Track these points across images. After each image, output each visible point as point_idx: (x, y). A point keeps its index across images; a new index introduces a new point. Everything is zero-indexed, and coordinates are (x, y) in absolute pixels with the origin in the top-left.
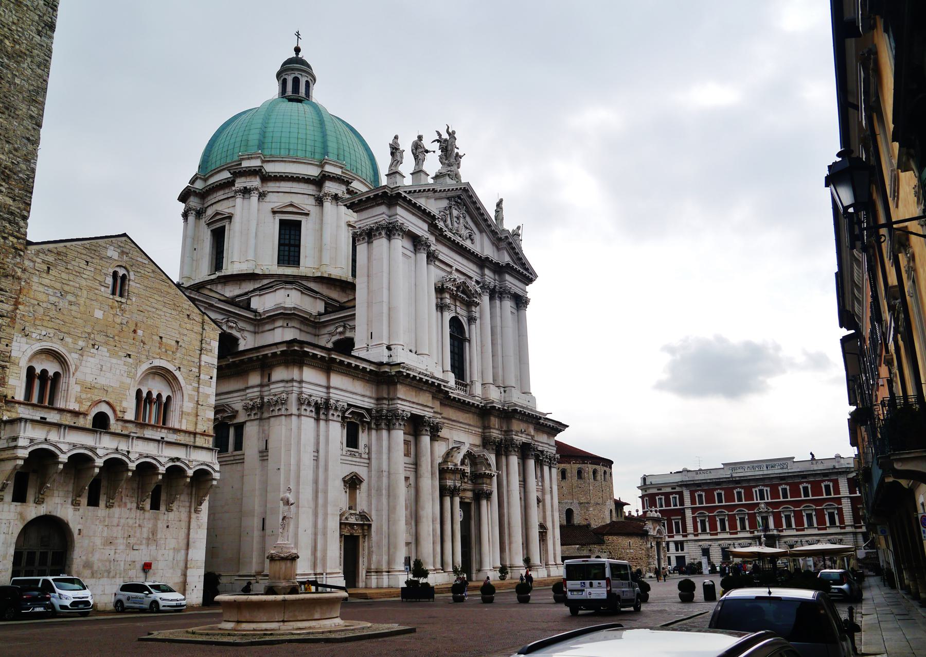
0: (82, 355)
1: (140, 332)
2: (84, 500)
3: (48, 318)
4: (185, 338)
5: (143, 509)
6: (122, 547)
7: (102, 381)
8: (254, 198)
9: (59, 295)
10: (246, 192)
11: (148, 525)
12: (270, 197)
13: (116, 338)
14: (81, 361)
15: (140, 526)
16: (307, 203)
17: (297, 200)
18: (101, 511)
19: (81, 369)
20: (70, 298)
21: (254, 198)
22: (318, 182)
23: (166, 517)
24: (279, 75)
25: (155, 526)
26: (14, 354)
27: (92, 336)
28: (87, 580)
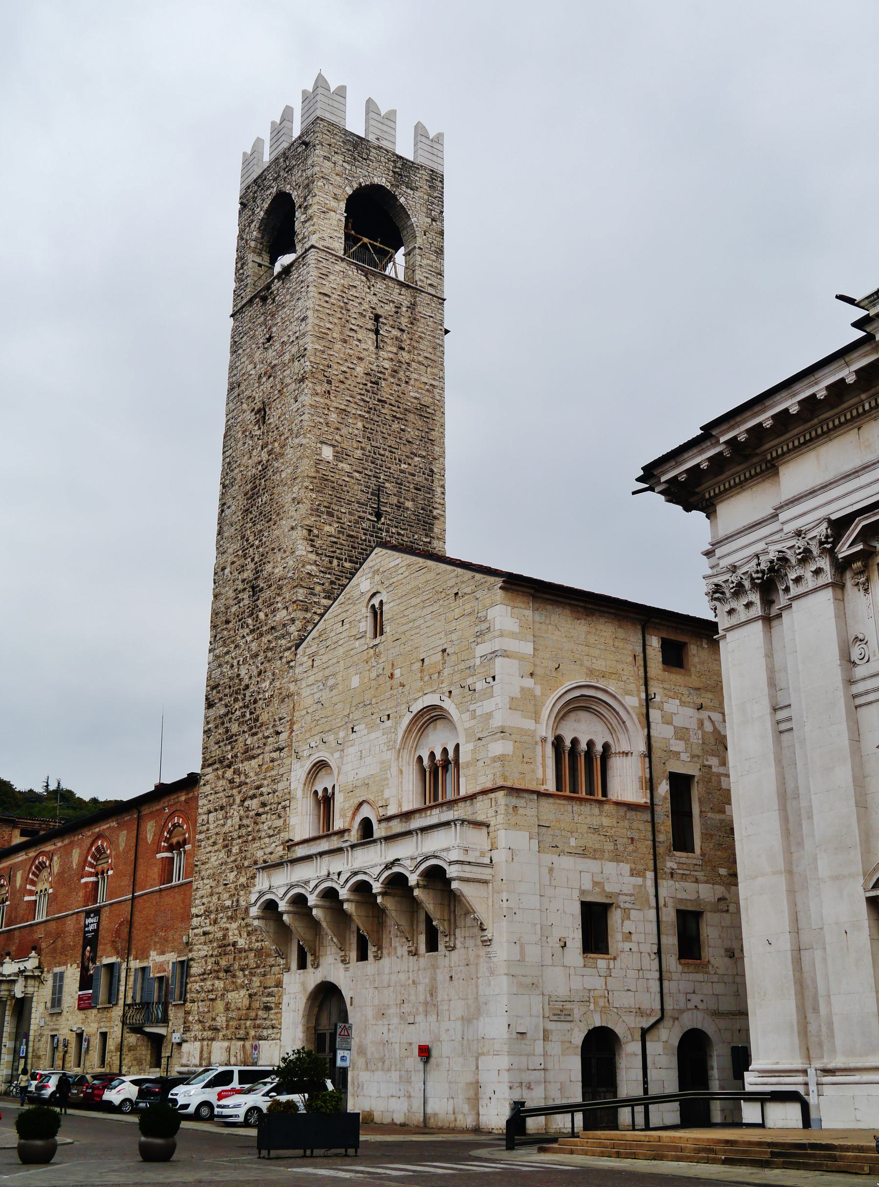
0: (343, 750)
1: (397, 673)
2: (353, 955)
3: (314, 723)
4: (454, 636)
5: (414, 953)
6: (395, 1021)
7: (363, 773)
9: (321, 687)
11: (424, 980)
13: (374, 701)
14: (341, 757)
15: (414, 982)
18: (370, 965)
19: (345, 768)
20: (331, 682)
23: (447, 959)
25: (434, 979)
26: (292, 788)
27: (351, 717)
28: (362, 1073)
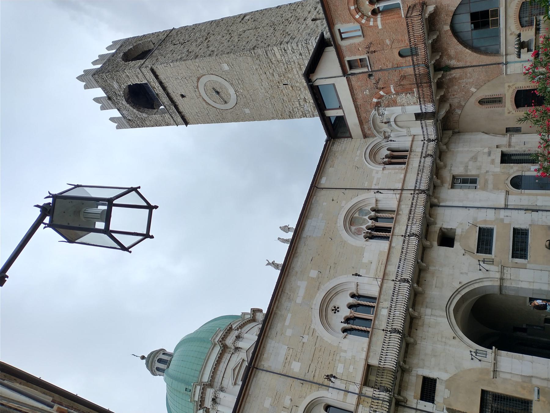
8: (221, 395)
10: (214, 400)
12: (225, 384)
16: (236, 359)
17: (232, 365)
21: (221, 395)
22: (225, 348)
24: (154, 374)
